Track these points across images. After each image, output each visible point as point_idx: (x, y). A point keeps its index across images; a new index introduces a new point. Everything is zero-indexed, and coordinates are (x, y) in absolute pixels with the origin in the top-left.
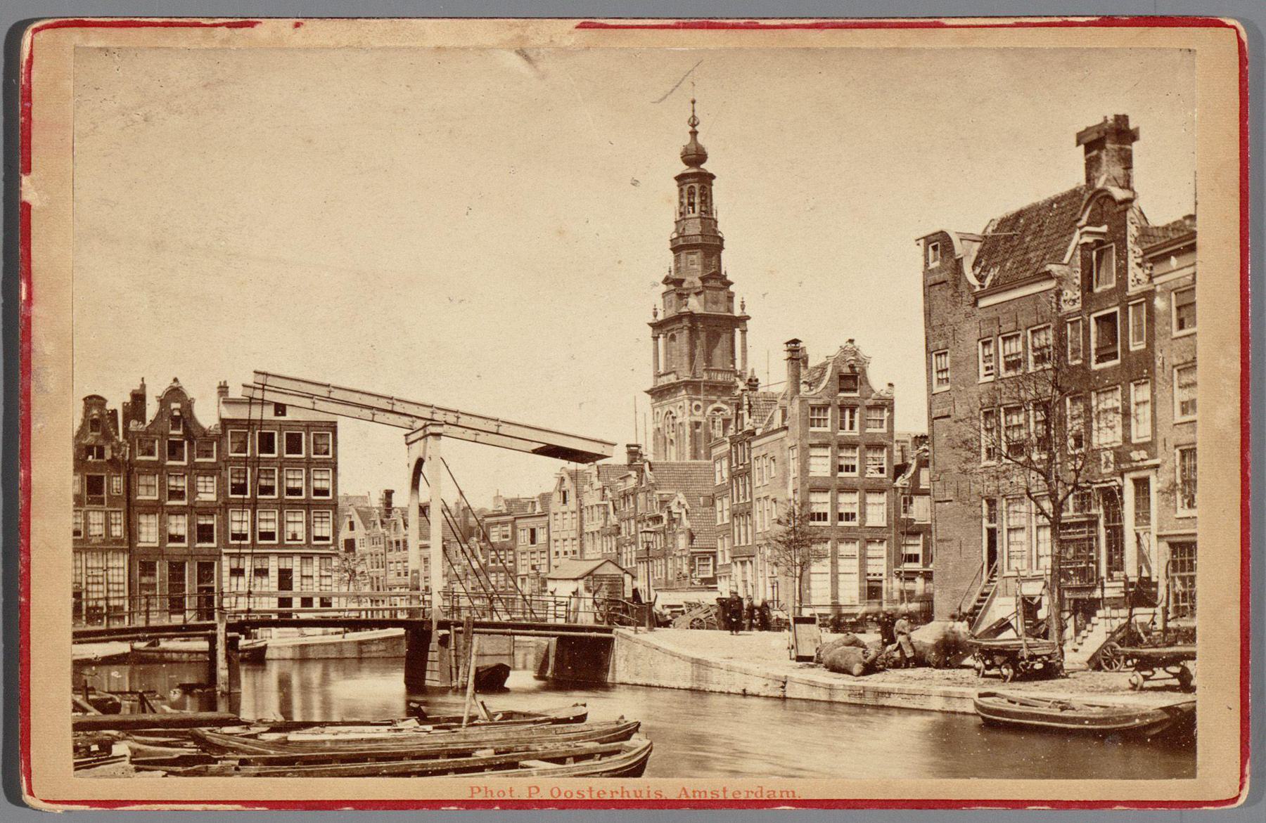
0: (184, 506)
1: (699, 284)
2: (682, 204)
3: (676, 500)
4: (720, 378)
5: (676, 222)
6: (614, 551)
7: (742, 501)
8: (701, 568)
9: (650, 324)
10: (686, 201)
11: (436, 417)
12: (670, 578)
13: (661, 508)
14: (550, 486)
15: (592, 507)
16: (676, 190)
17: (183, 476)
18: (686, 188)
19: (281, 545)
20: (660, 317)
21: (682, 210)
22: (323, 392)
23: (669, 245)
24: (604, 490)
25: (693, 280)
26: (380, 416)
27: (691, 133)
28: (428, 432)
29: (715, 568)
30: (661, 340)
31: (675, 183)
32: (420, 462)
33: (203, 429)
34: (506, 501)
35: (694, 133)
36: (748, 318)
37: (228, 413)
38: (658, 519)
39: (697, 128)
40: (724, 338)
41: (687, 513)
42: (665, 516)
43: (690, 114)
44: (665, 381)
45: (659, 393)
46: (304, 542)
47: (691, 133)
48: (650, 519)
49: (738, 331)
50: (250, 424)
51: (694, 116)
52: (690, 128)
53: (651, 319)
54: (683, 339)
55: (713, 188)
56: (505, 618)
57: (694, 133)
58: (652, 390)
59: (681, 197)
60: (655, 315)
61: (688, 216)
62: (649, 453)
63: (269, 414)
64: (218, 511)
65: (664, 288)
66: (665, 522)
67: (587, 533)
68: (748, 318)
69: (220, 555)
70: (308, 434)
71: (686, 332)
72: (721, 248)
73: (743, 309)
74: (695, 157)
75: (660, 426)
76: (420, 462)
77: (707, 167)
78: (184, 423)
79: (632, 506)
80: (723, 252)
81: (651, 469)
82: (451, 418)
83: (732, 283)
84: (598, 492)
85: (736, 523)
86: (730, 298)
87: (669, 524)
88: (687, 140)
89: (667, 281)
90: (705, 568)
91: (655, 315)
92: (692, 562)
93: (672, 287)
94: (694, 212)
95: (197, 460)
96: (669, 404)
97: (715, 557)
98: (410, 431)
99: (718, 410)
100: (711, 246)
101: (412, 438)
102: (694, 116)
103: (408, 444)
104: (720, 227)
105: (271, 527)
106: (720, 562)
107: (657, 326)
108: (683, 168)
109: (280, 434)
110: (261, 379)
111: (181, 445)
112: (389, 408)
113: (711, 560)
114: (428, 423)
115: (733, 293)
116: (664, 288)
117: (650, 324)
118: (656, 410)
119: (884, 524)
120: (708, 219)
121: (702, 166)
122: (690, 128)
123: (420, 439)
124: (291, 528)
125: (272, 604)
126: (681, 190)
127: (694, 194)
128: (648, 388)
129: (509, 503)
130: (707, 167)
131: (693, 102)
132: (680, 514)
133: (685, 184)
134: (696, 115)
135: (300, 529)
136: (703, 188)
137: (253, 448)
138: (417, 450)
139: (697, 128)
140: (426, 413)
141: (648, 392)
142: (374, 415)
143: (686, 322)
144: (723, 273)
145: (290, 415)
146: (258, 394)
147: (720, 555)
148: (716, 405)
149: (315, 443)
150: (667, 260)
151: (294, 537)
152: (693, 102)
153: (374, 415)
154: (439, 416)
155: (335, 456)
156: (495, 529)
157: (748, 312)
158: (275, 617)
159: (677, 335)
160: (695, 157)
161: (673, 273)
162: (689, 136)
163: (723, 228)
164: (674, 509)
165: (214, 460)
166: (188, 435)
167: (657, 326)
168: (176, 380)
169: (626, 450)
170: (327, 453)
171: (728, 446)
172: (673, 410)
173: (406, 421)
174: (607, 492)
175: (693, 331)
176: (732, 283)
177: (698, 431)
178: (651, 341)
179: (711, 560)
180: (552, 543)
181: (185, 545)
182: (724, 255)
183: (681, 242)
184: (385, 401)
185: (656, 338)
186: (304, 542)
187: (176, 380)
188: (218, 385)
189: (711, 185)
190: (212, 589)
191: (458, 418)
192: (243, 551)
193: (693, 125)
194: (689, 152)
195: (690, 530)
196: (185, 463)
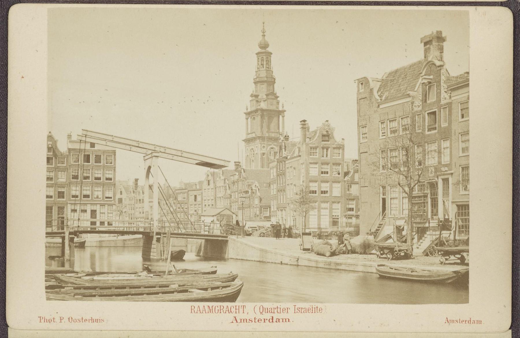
0: (52, 184)
1: (265, 97)
2: (258, 64)
3: (254, 185)
4: (273, 135)
5: (256, 72)
6: (229, 205)
7: (281, 185)
8: (264, 212)
9: (245, 113)
10: (260, 63)
11: (156, 149)
12: (251, 216)
13: (248, 188)
14: (203, 178)
15: (220, 187)
17: (53, 171)
18: (260, 58)
19: (92, 200)
20: (249, 110)
21: (258, 67)
22: (110, 138)
23: (253, 81)
24: (225, 180)
25: (262, 95)
26: (133, 149)
27: (262, 36)
28: (153, 155)
29: (270, 212)
30: (249, 120)
31: (256, 56)
32: (150, 168)
33: (61, 152)
34: (184, 184)
35: (264, 36)
36: (285, 111)
37: (71, 146)
38: (247, 192)
39: (265, 34)
40: (275, 120)
41: (259, 190)
42: (250, 191)
44: (250, 136)
45: (248, 141)
46: (101, 199)
47: (262, 36)
48: (244, 192)
49: (281, 117)
50: (80, 150)
51: (264, 29)
52: (262, 34)
53: (245, 111)
54: (258, 119)
55: (271, 58)
56: (184, 231)
57: (264, 36)
58: (245, 140)
59: (258, 61)
60: (247, 110)
61: (261, 69)
62: (244, 165)
63: (88, 146)
64: (66, 186)
65: (251, 98)
66: (250, 193)
67: (218, 197)
68: (285, 111)
69: (67, 204)
70: (104, 155)
71: (259, 117)
72: (274, 82)
73: (283, 107)
74: (264, 46)
75: (248, 154)
76: (150, 168)
77: (269, 49)
78: (53, 148)
79: (236, 187)
80: (275, 84)
81: (244, 172)
82: (162, 150)
83: (279, 97)
84: (223, 181)
85: (279, 194)
86: (278, 103)
87: (251, 194)
88: (261, 38)
89: (252, 96)
90: (266, 212)
91: (247, 110)
92: (261, 210)
93: (254, 98)
94: (263, 68)
95: (58, 165)
96: (252, 145)
97: (270, 208)
98: (146, 155)
99: (272, 148)
100: (271, 82)
101: (146, 158)
102: (264, 29)
103: (145, 160)
104: (274, 74)
105: (88, 193)
106: (272, 210)
107: (248, 114)
108: (259, 50)
109: (92, 155)
110: (85, 133)
111: (52, 158)
112: (137, 145)
113: (269, 209)
114: (153, 151)
115: (279, 101)
116: (251, 98)
117: (245, 113)
118: (247, 148)
120: (269, 69)
121: (267, 49)
122: (262, 34)
123: (150, 158)
124: (96, 194)
125: (88, 224)
126: (258, 59)
127: (263, 60)
128: (244, 139)
129: (186, 184)
130: (269, 49)
131: (264, 23)
132: (256, 190)
133: (260, 56)
134: (265, 28)
135: (100, 194)
136: (267, 58)
137: (81, 161)
138: (148, 163)
139: (265, 34)
140: (152, 148)
141: (243, 140)
142: (131, 148)
143: (259, 112)
144: (275, 93)
145: (97, 147)
146: (84, 139)
147: (272, 207)
148: (271, 146)
149: (106, 159)
150: (251, 88)
151: (97, 197)
152: (264, 23)
153: (131, 148)
154: (158, 149)
155: (115, 164)
156: (180, 195)
157: (285, 108)
158: (89, 229)
159: (256, 118)
160: (264, 46)
161: (254, 92)
162: (262, 37)
163: (275, 75)
164: (254, 188)
165: (65, 165)
166: (55, 155)
167: (248, 114)
168: (50, 132)
169: (234, 164)
170: (111, 163)
171: (276, 163)
172: (254, 148)
173: (144, 151)
174: (226, 181)
175: (262, 116)
176: (279, 97)
177: (264, 156)
178: (245, 120)
179: (269, 209)
180: (203, 201)
181: (53, 199)
182: (275, 85)
183: (258, 80)
184: (136, 142)
185: (247, 119)
186: (101, 199)
187: (50, 132)
188: (67, 135)
189: (271, 57)
190: (63, 218)
191: (165, 150)
192: (76, 202)
193: (263, 33)
195: (260, 196)
196: (53, 166)
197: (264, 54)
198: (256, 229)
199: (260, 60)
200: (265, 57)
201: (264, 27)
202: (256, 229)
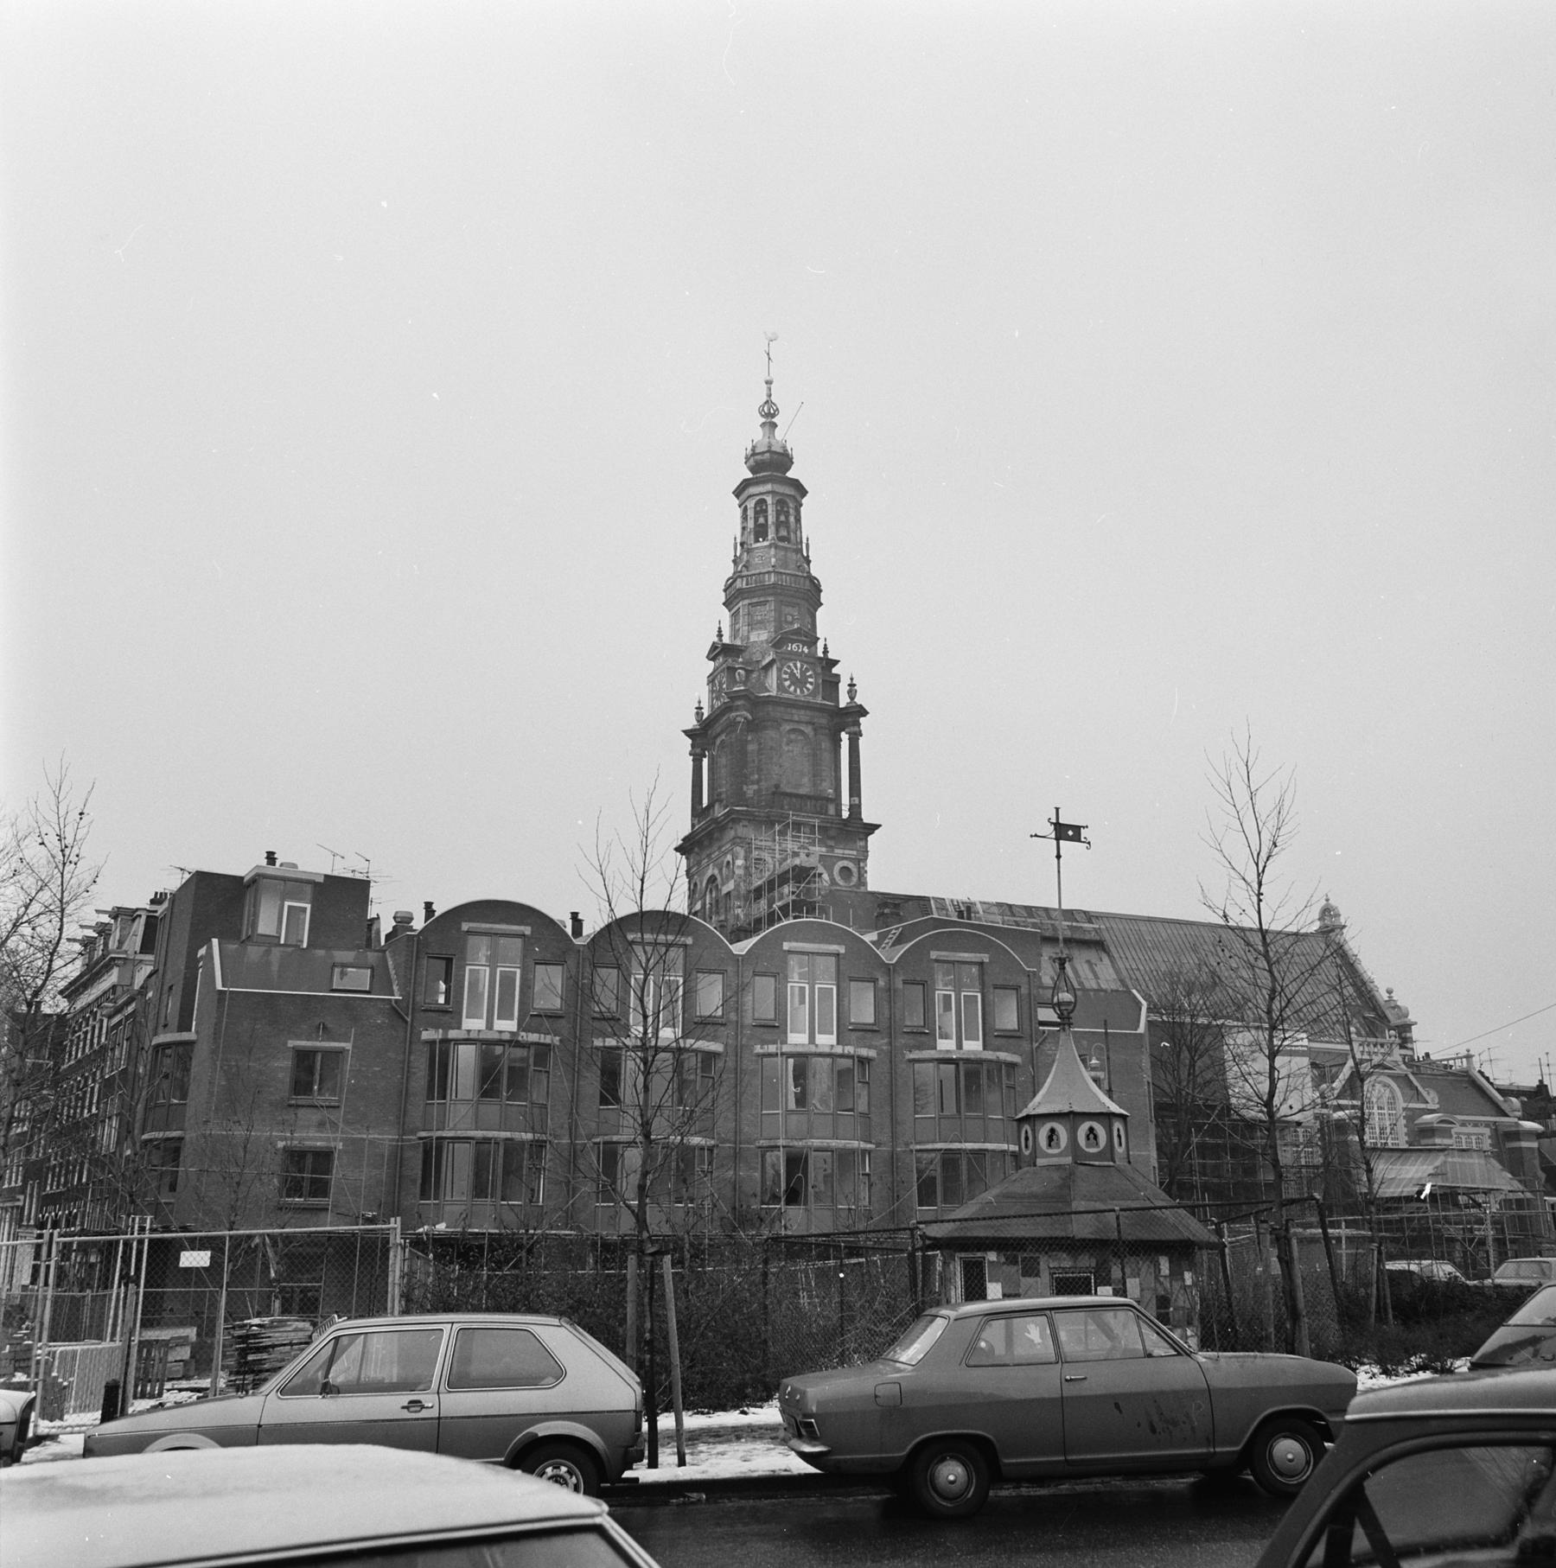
10: (751, 524)
16: (739, 512)
18: (751, 504)
27: (763, 425)
39: (774, 420)
43: (765, 398)
59: (745, 517)
68: (863, 712)
73: (852, 698)
88: (758, 435)
102: (767, 402)
127: (766, 511)
131: (769, 383)
134: (773, 398)
139: (774, 420)
152: (769, 383)
194: (757, 451)
197: (769, 487)
199: (751, 513)
200: (769, 499)
201: (770, 395)
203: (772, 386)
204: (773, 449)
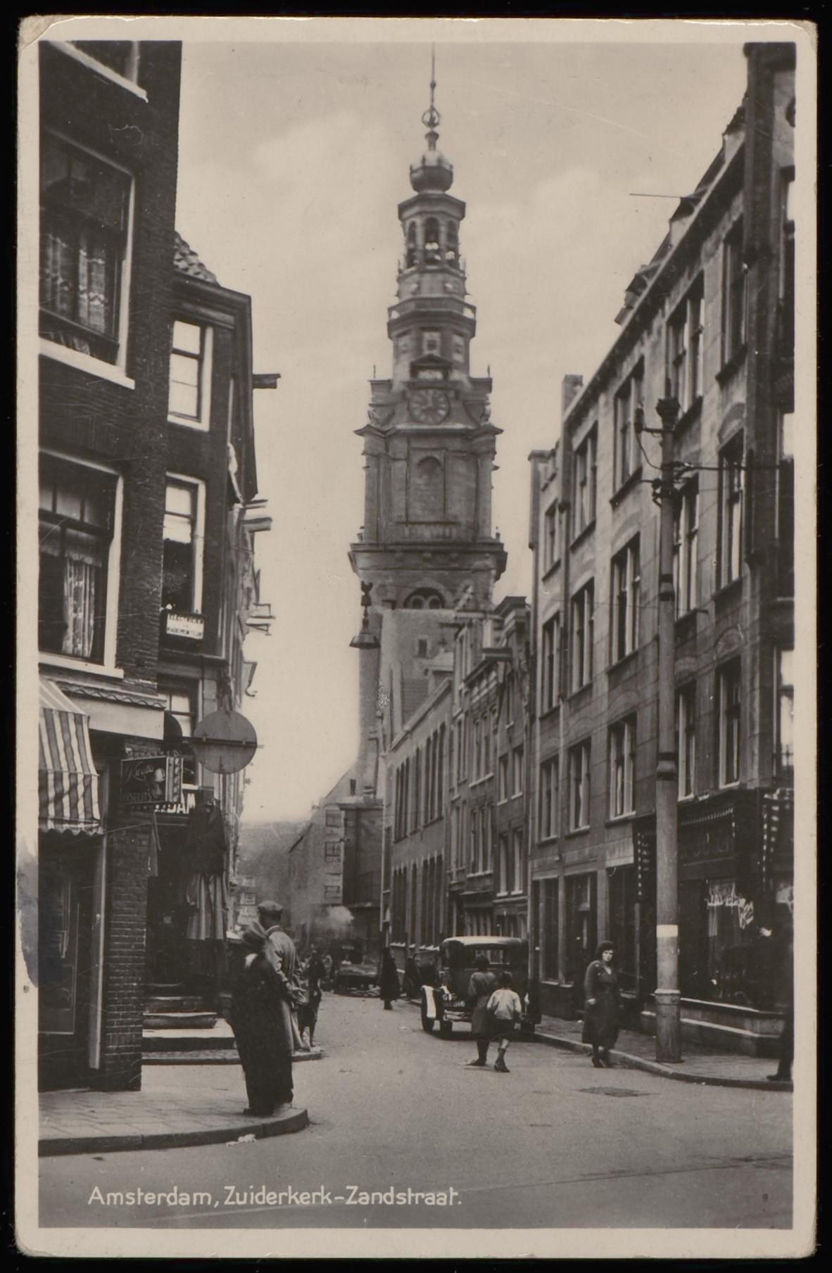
35: (433, 137)
39: (437, 129)
51: (432, 109)
52: (428, 130)
57: (433, 137)
102: (432, 109)
119: (143, 1067)
122: (428, 130)
131: (433, 85)
134: (436, 106)
139: (437, 129)
152: (433, 85)
162: (425, 143)
193: (432, 123)
197: (416, 209)
198: (480, 865)
201: (433, 100)
202: (480, 865)
203: (436, 89)
204: (427, 164)
